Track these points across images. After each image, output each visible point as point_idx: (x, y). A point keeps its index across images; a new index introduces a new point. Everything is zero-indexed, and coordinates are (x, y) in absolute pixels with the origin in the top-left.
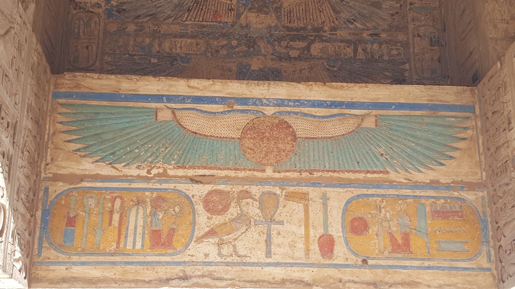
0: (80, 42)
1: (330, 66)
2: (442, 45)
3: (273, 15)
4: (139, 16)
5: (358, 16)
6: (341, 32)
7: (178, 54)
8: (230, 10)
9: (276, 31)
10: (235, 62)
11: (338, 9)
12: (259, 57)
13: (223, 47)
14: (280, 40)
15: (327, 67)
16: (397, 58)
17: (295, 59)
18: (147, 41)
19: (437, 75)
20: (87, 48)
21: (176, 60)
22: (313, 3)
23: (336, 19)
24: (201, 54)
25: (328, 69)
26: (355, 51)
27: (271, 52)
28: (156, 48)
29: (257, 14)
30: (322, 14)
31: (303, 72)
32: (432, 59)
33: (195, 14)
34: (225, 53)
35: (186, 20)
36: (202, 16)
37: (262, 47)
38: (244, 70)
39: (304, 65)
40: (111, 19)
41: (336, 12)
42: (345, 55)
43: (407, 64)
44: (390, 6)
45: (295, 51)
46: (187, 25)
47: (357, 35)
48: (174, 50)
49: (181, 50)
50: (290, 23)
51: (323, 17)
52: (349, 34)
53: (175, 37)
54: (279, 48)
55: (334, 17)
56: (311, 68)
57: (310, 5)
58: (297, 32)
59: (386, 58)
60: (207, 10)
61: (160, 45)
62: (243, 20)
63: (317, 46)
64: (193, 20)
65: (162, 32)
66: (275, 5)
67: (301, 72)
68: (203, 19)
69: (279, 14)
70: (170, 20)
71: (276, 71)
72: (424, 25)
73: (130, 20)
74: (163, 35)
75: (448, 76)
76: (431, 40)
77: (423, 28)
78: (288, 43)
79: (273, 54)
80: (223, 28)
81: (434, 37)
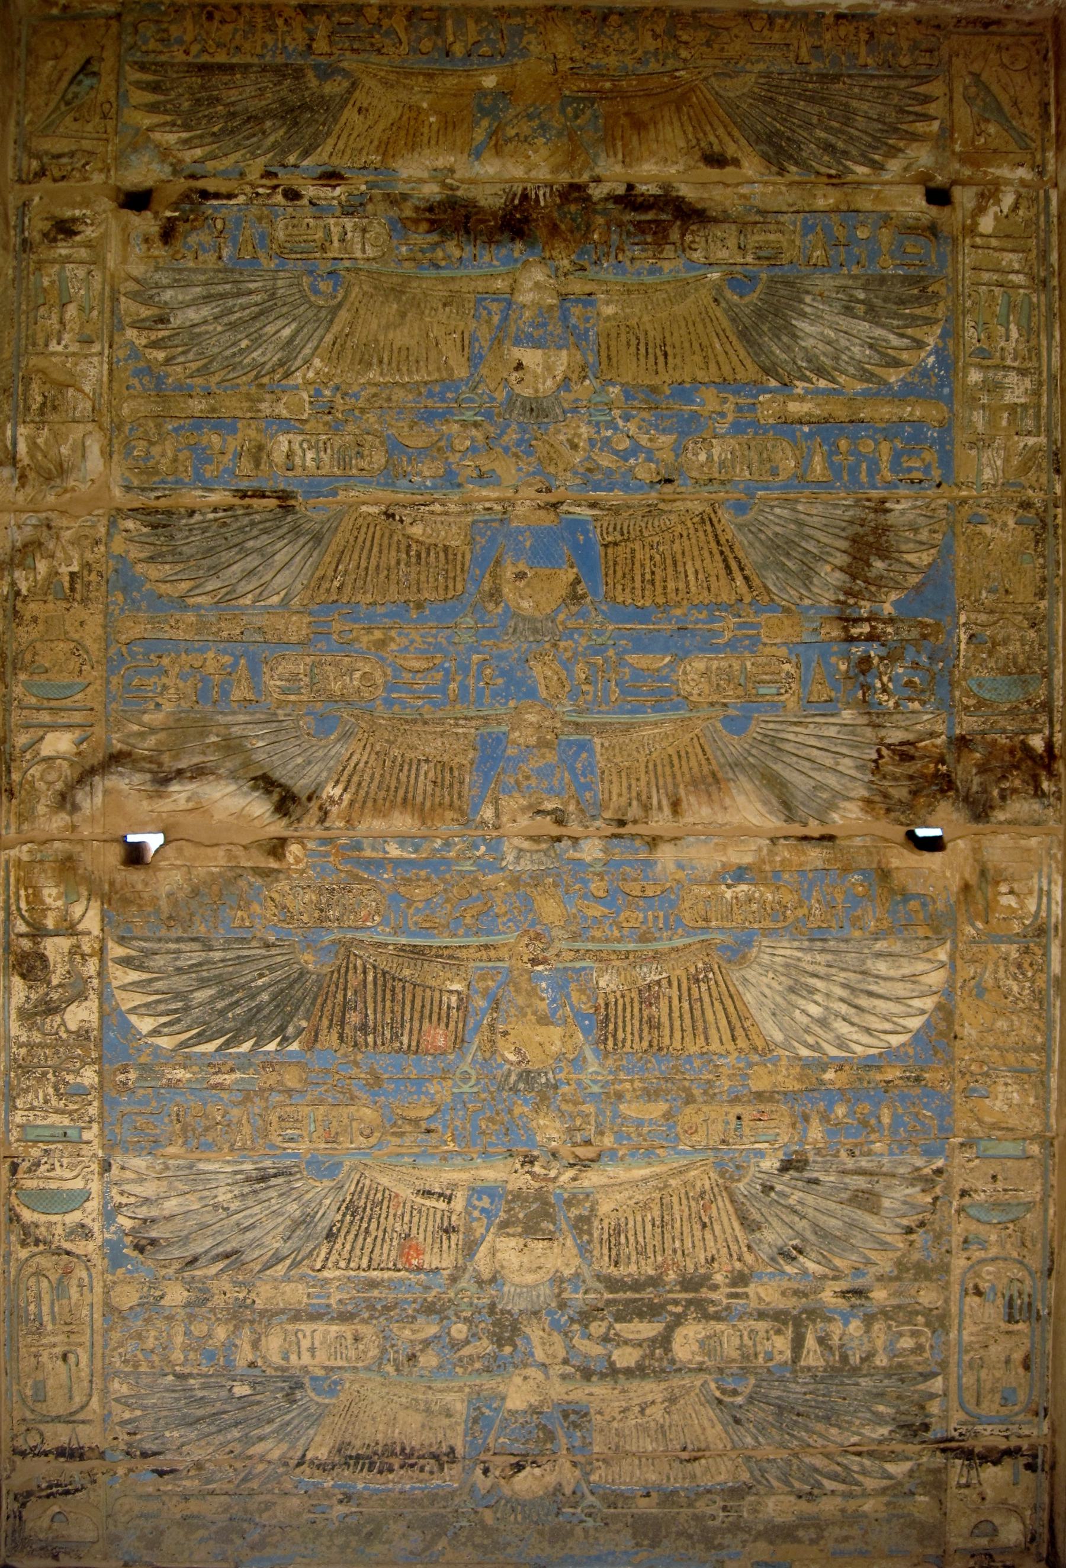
0: (44, 1341)
1: (724, 1392)
2: (1039, 1317)
3: (569, 1242)
4: (195, 1259)
5: (812, 1238)
6: (760, 1290)
7: (305, 1369)
8: (446, 1231)
9: (576, 1291)
10: (461, 1390)
11: (757, 1217)
12: (531, 1372)
13: (427, 1343)
14: (586, 1317)
15: (718, 1394)
16: (912, 1359)
17: (628, 1372)
18: (221, 1333)
19: (1017, 1408)
20: (65, 1357)
21: (300, 1386)
22: (684, 1201)
23: (749, 1247)
24: (368, 1369)
25: (720, 1402)
26: (798, 1344)
27: (562, 1354)
28: (245, 1354)
29: (522, 1241)
30: (708, 1236)
31: (648, 1412)
32: (1008, 1361)
33: (348, 1247)
34: (434, 1362)
35: (323, 1267)
36: (367, 1252)
37: (536, 1341)
38: (487, 1412)
39: (651, 1390)
40: (120, 1271)
41: (749, 1225)
42: (769, 1357)
43: (940, 1378)
44: (905, 1203)
45: (628, 1350)
46: (327, 1281)
47: (806, 1295)
48: (293, 1358)
49: (313, 1356)
50: (616, 1264)
51: (710, 1243)
52: (783, 1294)
53: (296, 1317)
54: (586, 1342)
55: (743, 1243)
56: (672, 1400)
57: (676, 1207)
58: (637, 1291)
59: (881, 1360)
60: (380, 1234)
61: (255, 1345)
62: (482, 1262)
63: (691, 1334)
64: (343, 1264)
65: (260, 1305)
66: (574, 1212)
67: (642, 1411)
68: (370, 1260)
69: (586, 1237)
70: (280, 1269)
71: (575, 1412)
72: (994, 1259)
73: (170, 1271)
74: (263, 1313)
75: (1046, 1410)
76: (1010, 1304)
77: (991, 1269)
78: (610, 1327)
79: (566, 1362)
80: (427, 1288)
81: (1020, 1294)
